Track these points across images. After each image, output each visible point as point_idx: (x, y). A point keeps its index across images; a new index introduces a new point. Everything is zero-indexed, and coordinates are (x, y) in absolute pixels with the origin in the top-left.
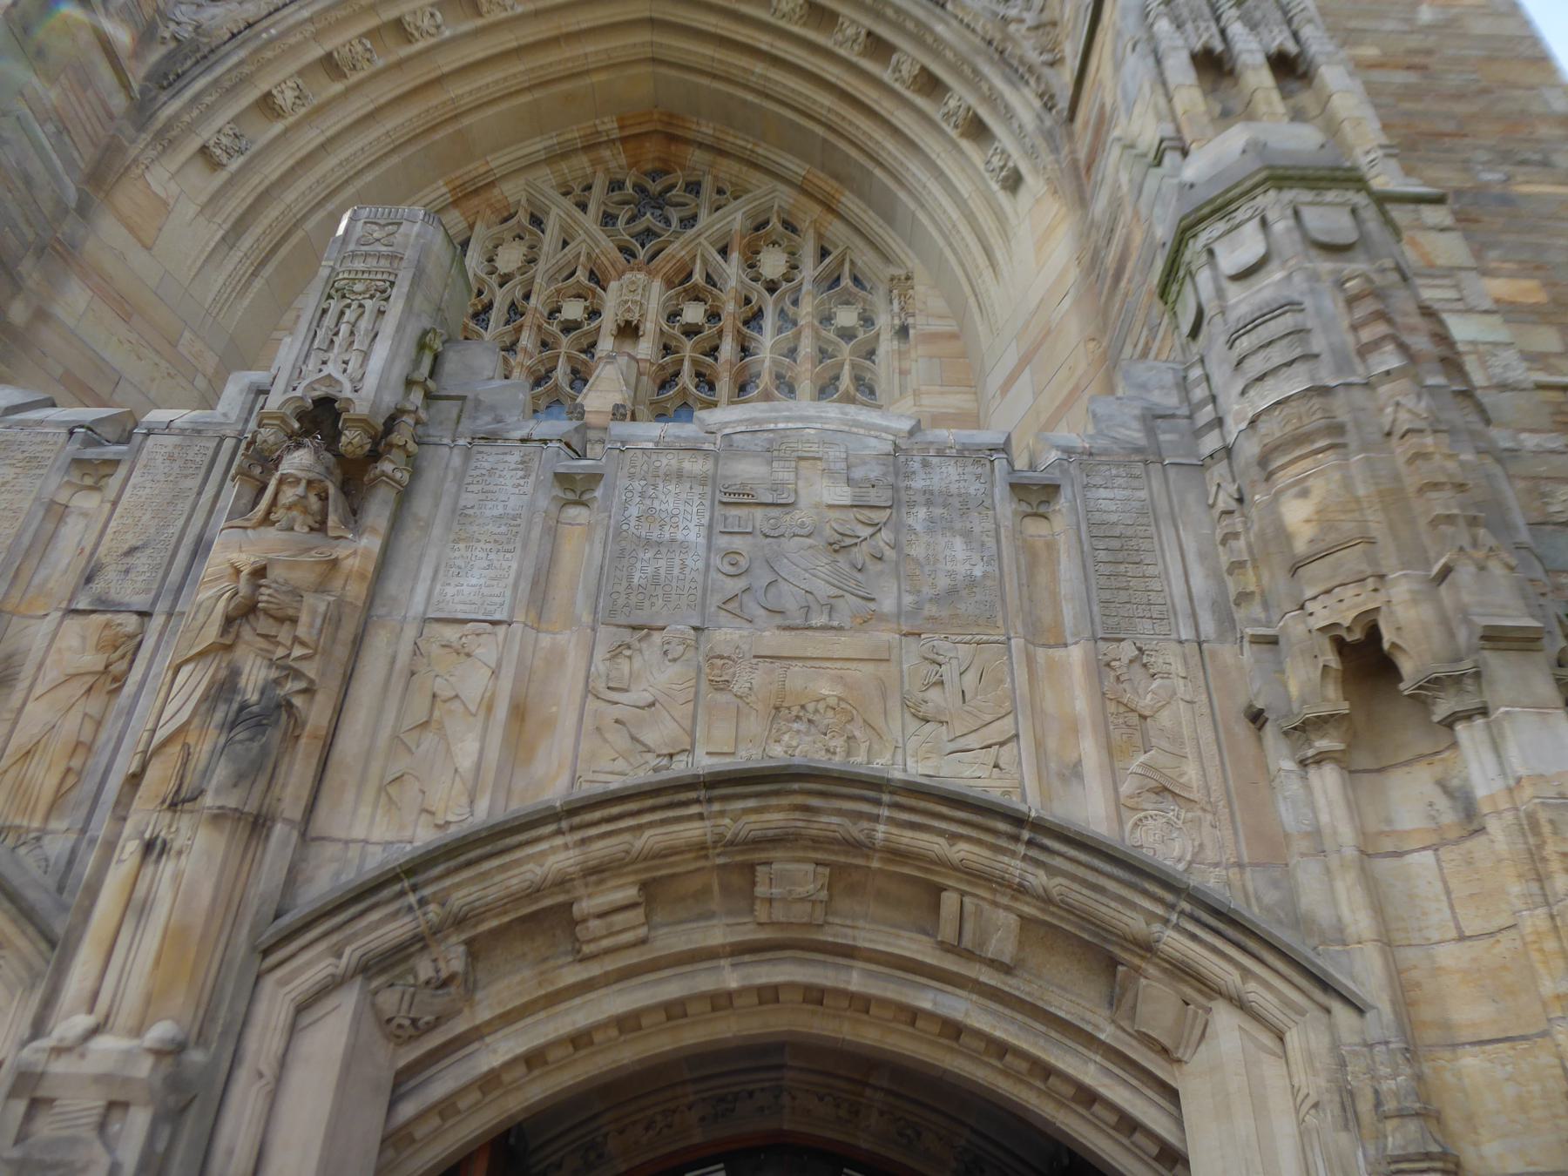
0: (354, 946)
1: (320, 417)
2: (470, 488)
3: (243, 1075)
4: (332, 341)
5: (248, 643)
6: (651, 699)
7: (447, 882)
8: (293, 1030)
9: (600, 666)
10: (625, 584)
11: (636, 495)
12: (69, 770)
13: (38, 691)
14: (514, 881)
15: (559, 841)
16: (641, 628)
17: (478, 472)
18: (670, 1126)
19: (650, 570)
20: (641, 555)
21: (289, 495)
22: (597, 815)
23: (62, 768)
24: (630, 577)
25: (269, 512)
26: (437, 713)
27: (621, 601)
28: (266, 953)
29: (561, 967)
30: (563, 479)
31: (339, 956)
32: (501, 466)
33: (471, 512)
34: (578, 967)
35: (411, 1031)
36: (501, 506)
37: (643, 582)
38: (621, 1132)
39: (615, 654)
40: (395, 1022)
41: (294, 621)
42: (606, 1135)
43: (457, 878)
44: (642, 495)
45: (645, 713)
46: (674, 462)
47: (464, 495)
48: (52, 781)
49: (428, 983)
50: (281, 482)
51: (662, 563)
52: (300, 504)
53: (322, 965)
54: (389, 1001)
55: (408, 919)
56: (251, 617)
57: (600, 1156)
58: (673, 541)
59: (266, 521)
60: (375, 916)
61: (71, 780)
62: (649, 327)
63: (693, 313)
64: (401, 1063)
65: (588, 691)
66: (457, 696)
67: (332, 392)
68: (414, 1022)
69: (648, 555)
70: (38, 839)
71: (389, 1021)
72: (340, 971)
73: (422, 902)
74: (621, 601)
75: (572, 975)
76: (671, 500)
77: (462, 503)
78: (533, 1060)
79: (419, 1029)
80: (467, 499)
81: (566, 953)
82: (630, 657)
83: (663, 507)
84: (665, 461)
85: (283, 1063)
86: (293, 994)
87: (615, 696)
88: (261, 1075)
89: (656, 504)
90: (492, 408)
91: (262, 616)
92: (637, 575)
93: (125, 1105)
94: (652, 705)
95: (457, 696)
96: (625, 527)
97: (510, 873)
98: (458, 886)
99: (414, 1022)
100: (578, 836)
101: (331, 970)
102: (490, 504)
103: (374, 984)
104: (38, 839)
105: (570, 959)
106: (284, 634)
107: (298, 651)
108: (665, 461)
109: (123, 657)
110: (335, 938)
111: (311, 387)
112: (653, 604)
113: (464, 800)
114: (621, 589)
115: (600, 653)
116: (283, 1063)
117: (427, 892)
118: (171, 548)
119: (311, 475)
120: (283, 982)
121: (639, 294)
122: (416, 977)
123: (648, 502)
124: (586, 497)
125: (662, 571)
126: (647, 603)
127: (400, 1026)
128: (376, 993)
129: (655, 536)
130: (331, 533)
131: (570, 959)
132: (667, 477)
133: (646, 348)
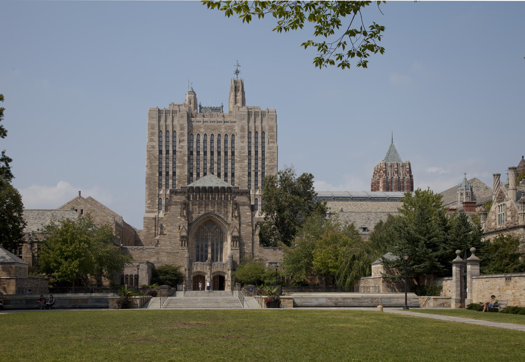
121: (210, 234)
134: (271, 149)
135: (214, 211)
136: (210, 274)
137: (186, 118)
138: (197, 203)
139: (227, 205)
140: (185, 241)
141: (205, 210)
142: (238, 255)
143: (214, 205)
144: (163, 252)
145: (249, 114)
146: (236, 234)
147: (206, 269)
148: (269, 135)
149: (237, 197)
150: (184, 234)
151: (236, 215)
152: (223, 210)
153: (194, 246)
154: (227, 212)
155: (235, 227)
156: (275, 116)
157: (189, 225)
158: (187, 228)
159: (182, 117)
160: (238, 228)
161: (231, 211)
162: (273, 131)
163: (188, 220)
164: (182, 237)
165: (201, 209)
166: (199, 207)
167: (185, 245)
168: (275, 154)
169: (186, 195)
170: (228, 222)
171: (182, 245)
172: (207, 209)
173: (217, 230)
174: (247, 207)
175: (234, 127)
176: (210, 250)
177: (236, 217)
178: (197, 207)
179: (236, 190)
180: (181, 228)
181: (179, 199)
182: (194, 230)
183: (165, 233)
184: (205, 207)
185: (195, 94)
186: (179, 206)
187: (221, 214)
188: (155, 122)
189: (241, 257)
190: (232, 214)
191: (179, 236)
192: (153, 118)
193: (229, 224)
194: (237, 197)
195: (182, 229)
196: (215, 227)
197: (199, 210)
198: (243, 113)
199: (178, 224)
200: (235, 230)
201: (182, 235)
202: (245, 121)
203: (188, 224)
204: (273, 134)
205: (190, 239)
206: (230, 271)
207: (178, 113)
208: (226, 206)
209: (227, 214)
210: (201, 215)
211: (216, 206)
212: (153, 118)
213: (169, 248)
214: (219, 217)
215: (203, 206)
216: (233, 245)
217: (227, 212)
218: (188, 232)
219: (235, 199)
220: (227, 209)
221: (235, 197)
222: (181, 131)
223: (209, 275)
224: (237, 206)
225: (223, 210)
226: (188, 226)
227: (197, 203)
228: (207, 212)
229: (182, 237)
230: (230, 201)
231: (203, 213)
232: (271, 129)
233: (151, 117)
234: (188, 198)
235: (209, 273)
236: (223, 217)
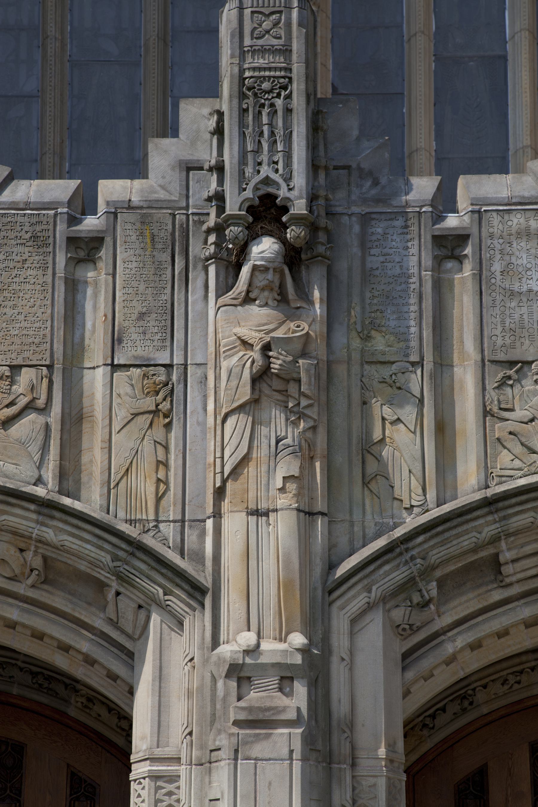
0: (378, 585)
1: (266, 213)
2: (373, 251)
3: (335, 659)
4: (259, 142)
5: (268, 396)
6: (531, 416)
7: (426, 546)
8: (352, 634)
9: (492, 394)
10: (500, 329)
11: (497, 252)
12: (159, 480)
13: (116, 427)
14: (466, 543)
15: (490, 518)
16: (515, 363)
17: (374, 238)
18: (519, 682)
19: (517, 316)
20: (508, 305)
21: (261, 280)
22: (513, 501)
23: (154, 480)
24: (503, 322)
25: (248, 292)
26: (387, 432)
27: (500, 342)
28: (330, 592)
29: (491, 590)
30: (439, 240)
31: (370, 591)
32: (391, 231)
33: (377, 273)
34: (500, 591)
35: (409, 632)
36: (398, 268)
37: (513, 326)
38: (485, 687)
39: (502, 384)
40: (402, 627)
41: (299, 381)
42: (474, 690)
43: (432, 543)
44: (501, 252)
45: (529, 427)
46: (522, 220)
47: (369, 259)
48: (151, 488)
49: (418, 604)
50: (255, 268)
51: (524, 310)
52: (269, 287)
53: (361, 597)
54: (398, 615)
55: (405, 569)
56: (265, 377)
57: (471, 703)
58: (530, 291)
59: (248, 300)
60: (387, 568)
61: (162, 487)
64: (404, 650)
65: (486, 413)
66: (399, 419)
67: (271, 190)
68: (411, 626)
69: (513, 304)
70: (156, 526)
71: (398, 626)
72: (372, 600)
73: (413, 558)
74: (500, 342)
75: (497, 596)
76: (524, 256)
77: (369, 265)
78: (476, 646)
79: (413, 629)
80: (373, 262)
81: (492, 582)
82: (512, 386)
83: (520, 262)
84: (515, 221)
85: (351, 653)
86: (349, 614)
87: (506, 415)
88: (343, 659)
89: (513, 260)
90: (370, 173)
91: (274, 377)
92: (508, 321)
93: (292, 679)
94: (532, 420)
95: (399, 419)
96: (493, 281)
97: (462, 539)
98: (433, 547)
99: (411, 626)
100: (502, 514)
101: (366, 600)
102: (389, 265)
103: (388, 606)
104: (156, 526)
105: (495, 585)
106: (292, 389)
107: (304, 402)
108: (515, 221)
109: (164, 399)
110: (365, 582)
111: (256, 188)
112: (522, 344)
113: (420, 491)
114: (498, 332)
115: (491, 385)
116: (351, 653)
117: (414, 552)
118: (169, 312)
119: (276, 264)
120: (342, 608)
122: (411, 601)
123: (507, 258)
124: (457, 252)
125: (525, 316)
126: (518, 344)
127: (404, 630)
128: (389, 611)
129: (516, 287)
130: (293, 305)
131: (495, 585)
132: (519, 235)
136: (319, 594)
147: (164, 397)
223: (254, 623)
235: (256, 551)
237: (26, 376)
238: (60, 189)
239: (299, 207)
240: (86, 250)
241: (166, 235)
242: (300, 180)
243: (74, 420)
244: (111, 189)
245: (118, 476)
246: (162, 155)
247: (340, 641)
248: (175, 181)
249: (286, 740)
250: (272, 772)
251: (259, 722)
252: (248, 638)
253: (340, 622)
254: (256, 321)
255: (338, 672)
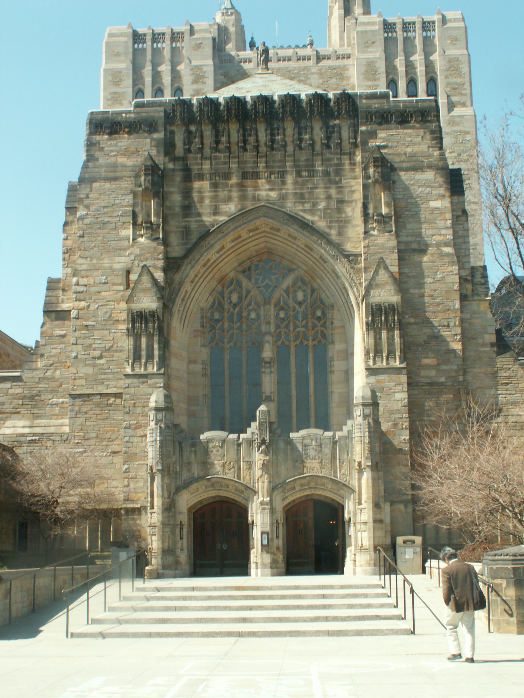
59: (261, 453)
62: (272, 321)
63: (282, 315)
133: (272, 329)
134: (458, 124)
135: (283, 198)
137: (208, 50)
138: (206, 166)
139: (339, 172)
140: (150, 337)
141: (243, 198)
142: (401, 396)
143: (283, 174)
144: (54, 392)
145: (388, 27)
146: (387, 295)
147: (250, 465)
148: (448, 84)
149: (382, 134)
150: (148, 302)
151: (384, 211)
152: (320, 192)
153: (198, 368)
154: (341, 202)
155: (381, 263)
156: (462, 31)
157: (171, 265)
158: (159, 276)
159: (198, 46)
160: (395, 269)
161: (359, 196)
162: (460, 74)
163: (165, 243)
164: (139, 318)
165: (223, 194)
166: (215, 186)
167: (150, 357)
168: (468, 137)
169: (159, 135)
170: (349, 247)
171: (137, 357)
172: (250, 191)
173: (300, 296)
174: (429, 175)
175: (345, 68)
176: (269, 383)
177: (383, 220)
178: (206, 184)
179: (375, 105)
180: (133, 277)
181: (127, 153)
182: (198, 290)
183: (65, 306)
184: (241, 186)
185: (237, 14)
186: (127, 184)
187: (312, 211)
188: (124, 65)
189: (414, 407)
190: (365, 206)
191: (124, 316)
192: (118, 54)
193: (352, 258)
194: (382, 134)
195: (137, 282)
196: (288, 281)
197: (215, 198)
198: (369, 28)
199: (121, 262)
200: (383, 276)
201: (137, 306)
202: (377, 53)
203: (167, 258)
204: (458, 80)
205: (180, 334)
206: (367, 477)
207: (187, 36)
208: (334, 177)
209: (339, 210)
210: (222, 219)
211: (290, 179)
212: (118, 54)
213: (78, 376)
214: (305, 226)
215: (234, 180)
216: (378, 351)
217: (341, 202)
218: (167, 293)
219: (372, 143)
220: (340, 188)
221: (373, 135)
222: (195, 87)
224: (386, 172)
225: (320, 192)
226: (165, 270)
227: (206, 166)
228: (249, 205)
229: (139, 318)
230: (351, 155)
231: (232, 208)
232: (453, 66)
233: (112, 53)
234: (168, 147)
236: (321, 224)
237: (232, 463)
238: (235, 436)
239: (268, 441)
240: (239, 445)
241: (250, 442)
242: (268, 437)
243: (239, 468)
244: (242, 436)
245: (245, 479)
246: (249, 430)
247: (274, 498)
248: (251, 435)
249: (267, 511)
250: (265, 515)
251: (264, 509)
252: (262, 499)
253: (274, 496)
254: (262, 457)
255: (274, 504)
